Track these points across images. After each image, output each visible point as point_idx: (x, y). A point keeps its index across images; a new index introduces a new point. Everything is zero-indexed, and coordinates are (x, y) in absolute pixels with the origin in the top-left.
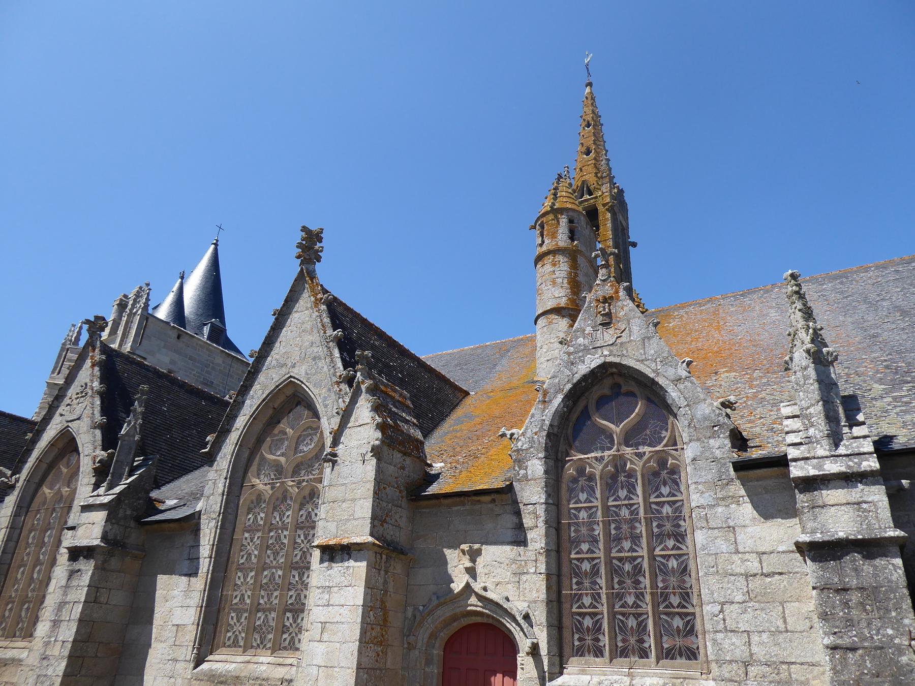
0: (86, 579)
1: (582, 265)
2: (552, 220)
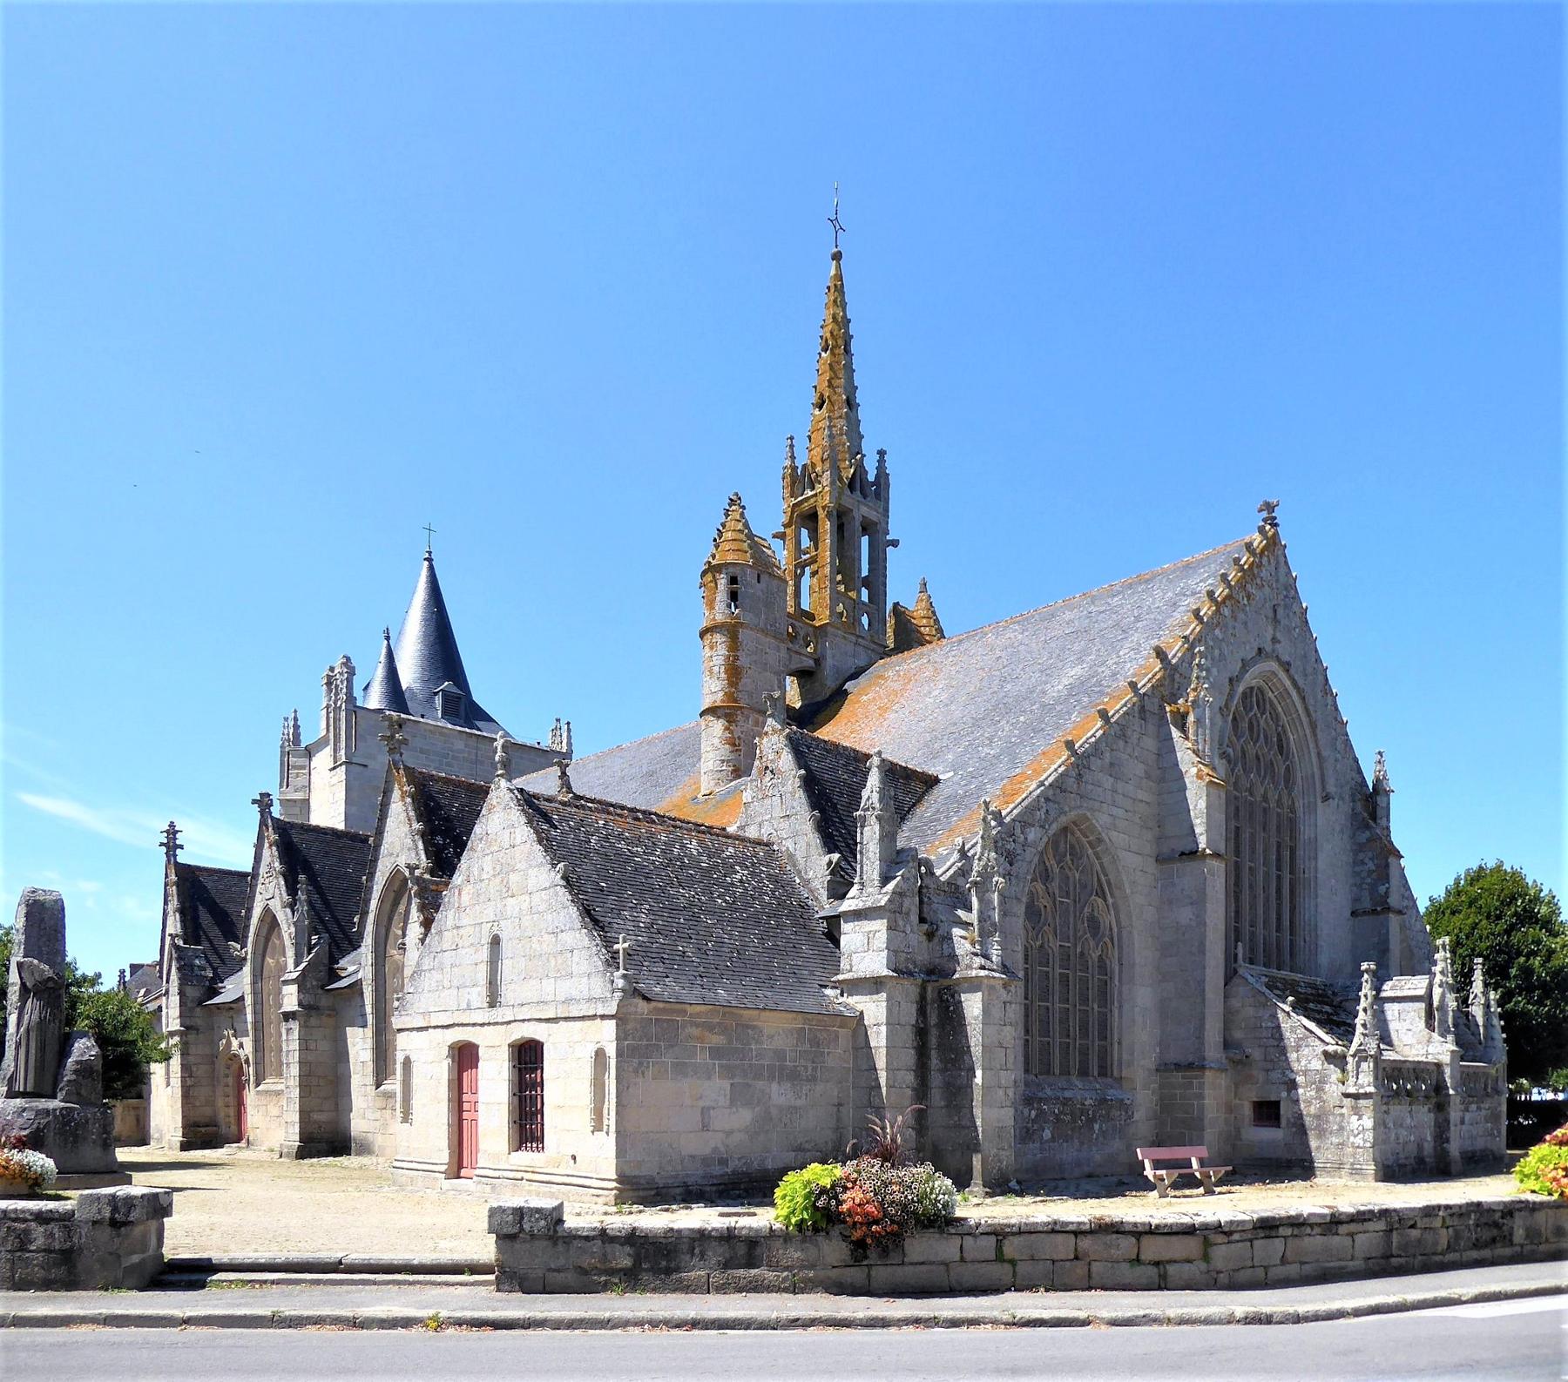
0: (296, 1035)
1: (745, 642)
2: (711, 582)
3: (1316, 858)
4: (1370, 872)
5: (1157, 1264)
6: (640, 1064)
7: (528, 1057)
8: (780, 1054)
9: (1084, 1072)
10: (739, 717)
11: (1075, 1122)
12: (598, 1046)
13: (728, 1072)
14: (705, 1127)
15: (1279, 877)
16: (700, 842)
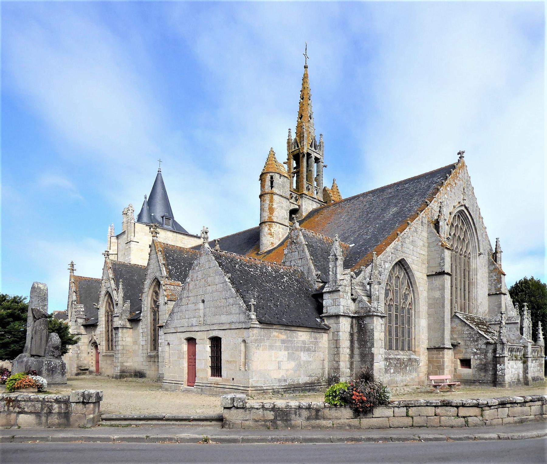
1: (275, 199)
3: (477, 275)
4: (495, 280)
5: (464, 417)
6: (258, 345)
7: (216, 342)
8: (304, 342)
9: (403, 349)
10: (273, 225)
11: (401, 367)
12: (243, 339)
13: (287, 348)
14: (279, 368)
15: (464, 281)
16: (272, 268)
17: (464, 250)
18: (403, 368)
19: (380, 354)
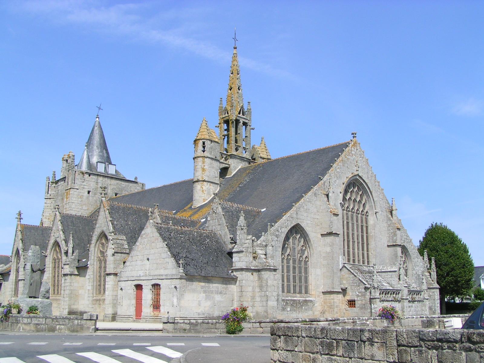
4: (392, 233)
9: (300, 292)
13: (205, 292)
17: (361, 210)
18: (299, 308)
19: (273, 296)
